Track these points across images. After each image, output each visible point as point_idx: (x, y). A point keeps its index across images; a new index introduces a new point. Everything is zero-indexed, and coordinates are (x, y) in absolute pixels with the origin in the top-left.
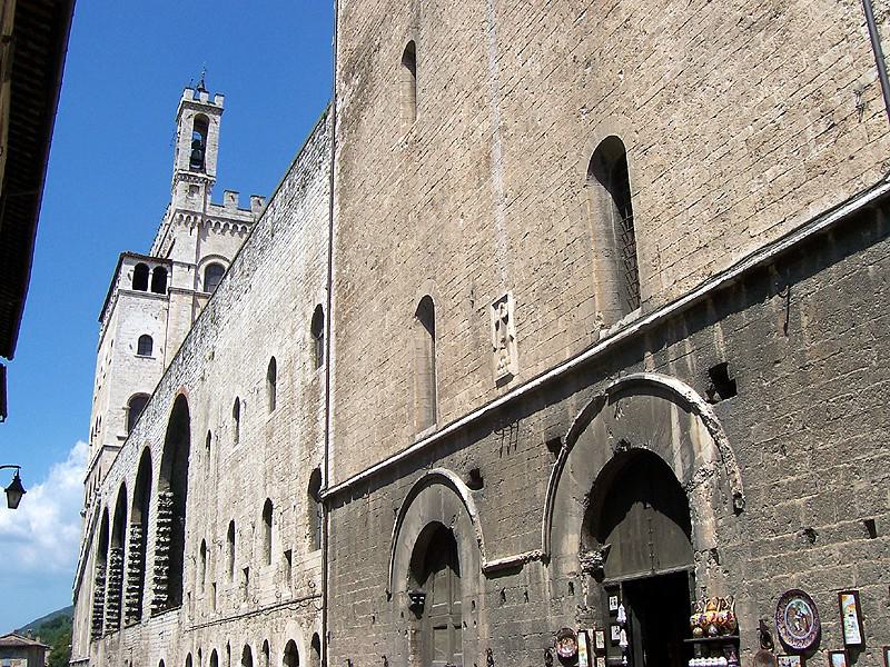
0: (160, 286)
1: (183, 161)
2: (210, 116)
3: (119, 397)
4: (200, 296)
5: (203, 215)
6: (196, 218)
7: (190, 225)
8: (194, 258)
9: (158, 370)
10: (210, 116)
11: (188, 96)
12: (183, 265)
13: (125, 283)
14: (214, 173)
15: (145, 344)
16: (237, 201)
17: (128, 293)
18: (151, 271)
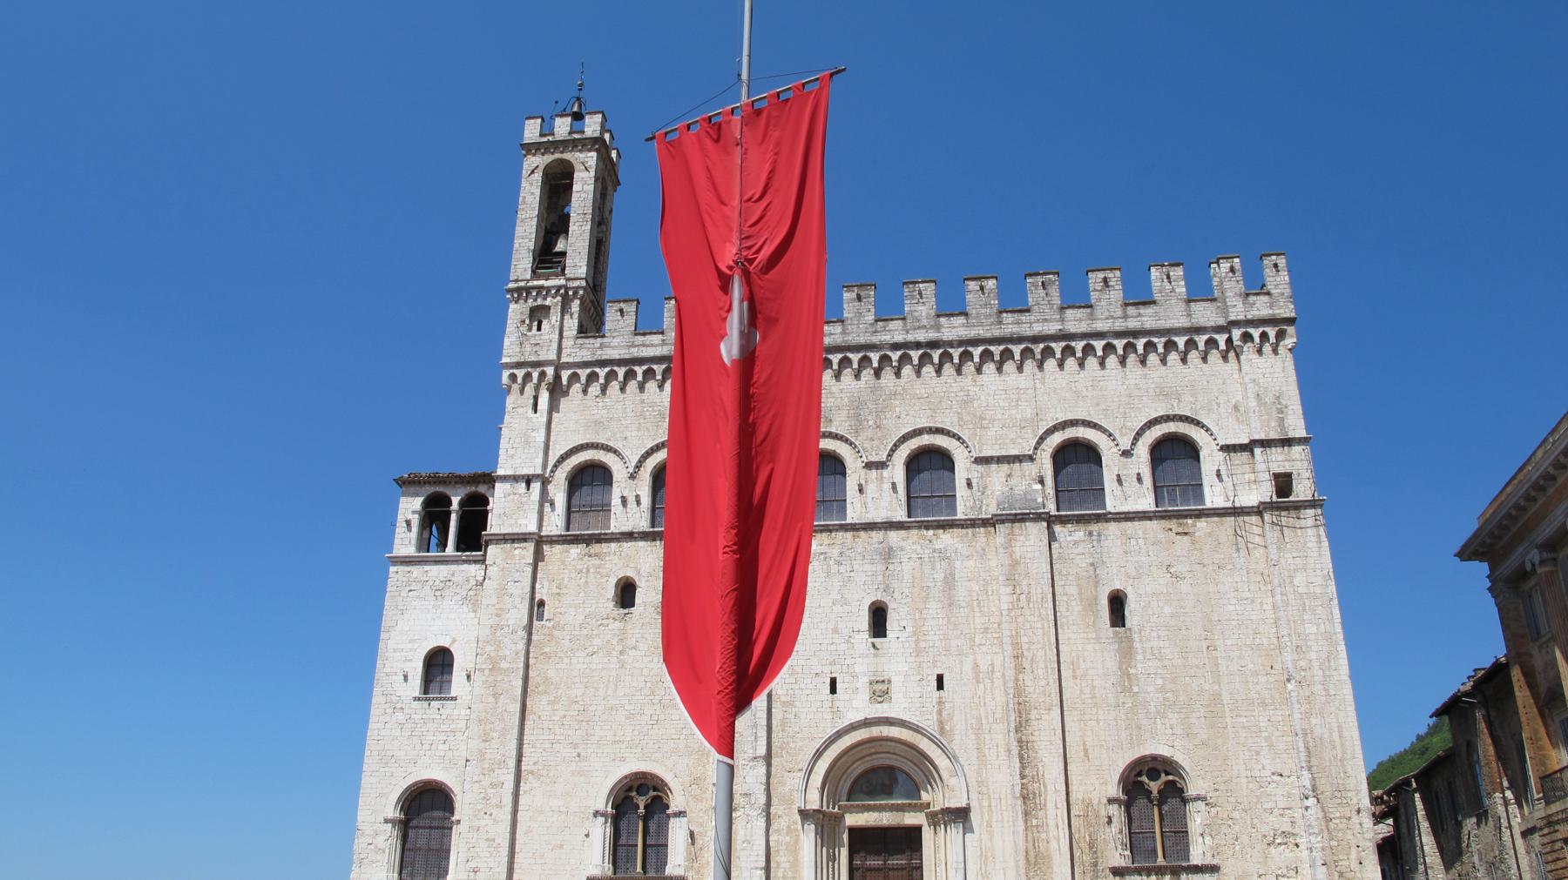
0: (473, 537)
1: (522, 264)
2: (575, 157)
3: (381, 795)
4: (553, 540)
5: (559, 367)
6: (543, 375)
7: (529, 389)
8: (539, 461)
9: (462, 724)
10: (575, 157)
11: (532, 131)
12: (515, 479)
13: (405, 542)
14: (582, 271)
15: (438, 664)
16: (630, 319)
17: (407, 561)
18: (455, 505)
